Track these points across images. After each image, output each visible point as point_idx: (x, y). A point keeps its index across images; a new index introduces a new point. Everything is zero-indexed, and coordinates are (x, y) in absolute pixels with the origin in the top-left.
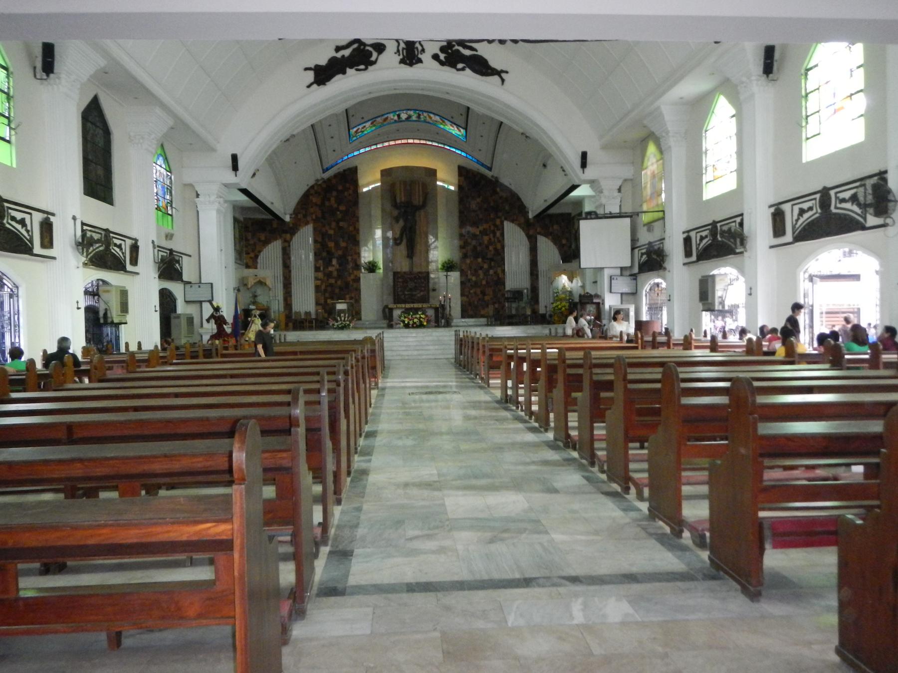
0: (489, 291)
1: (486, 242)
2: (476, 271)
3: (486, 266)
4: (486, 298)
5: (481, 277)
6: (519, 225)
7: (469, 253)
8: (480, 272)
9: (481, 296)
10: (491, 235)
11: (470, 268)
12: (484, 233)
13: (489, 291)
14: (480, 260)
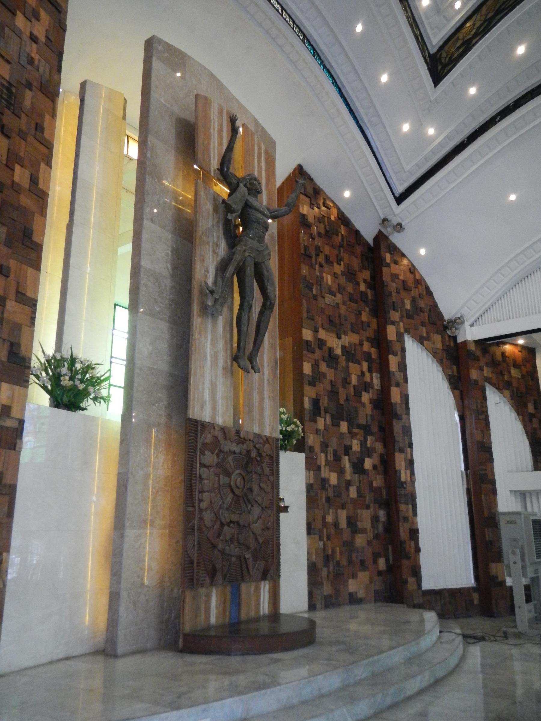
0: (365, 518)
1: (354, 380)
2: (337, 458)
3: (356, 446)
4: (360, 540)
5: (348, 476)
6: (434, 353)
7: (324, 402)
8: (346, 462)
9: (346, 536)
10: (365, 365)
11: (325, 446)
12: (349, 353)
13: (365, 518)
14: (344, 426)
